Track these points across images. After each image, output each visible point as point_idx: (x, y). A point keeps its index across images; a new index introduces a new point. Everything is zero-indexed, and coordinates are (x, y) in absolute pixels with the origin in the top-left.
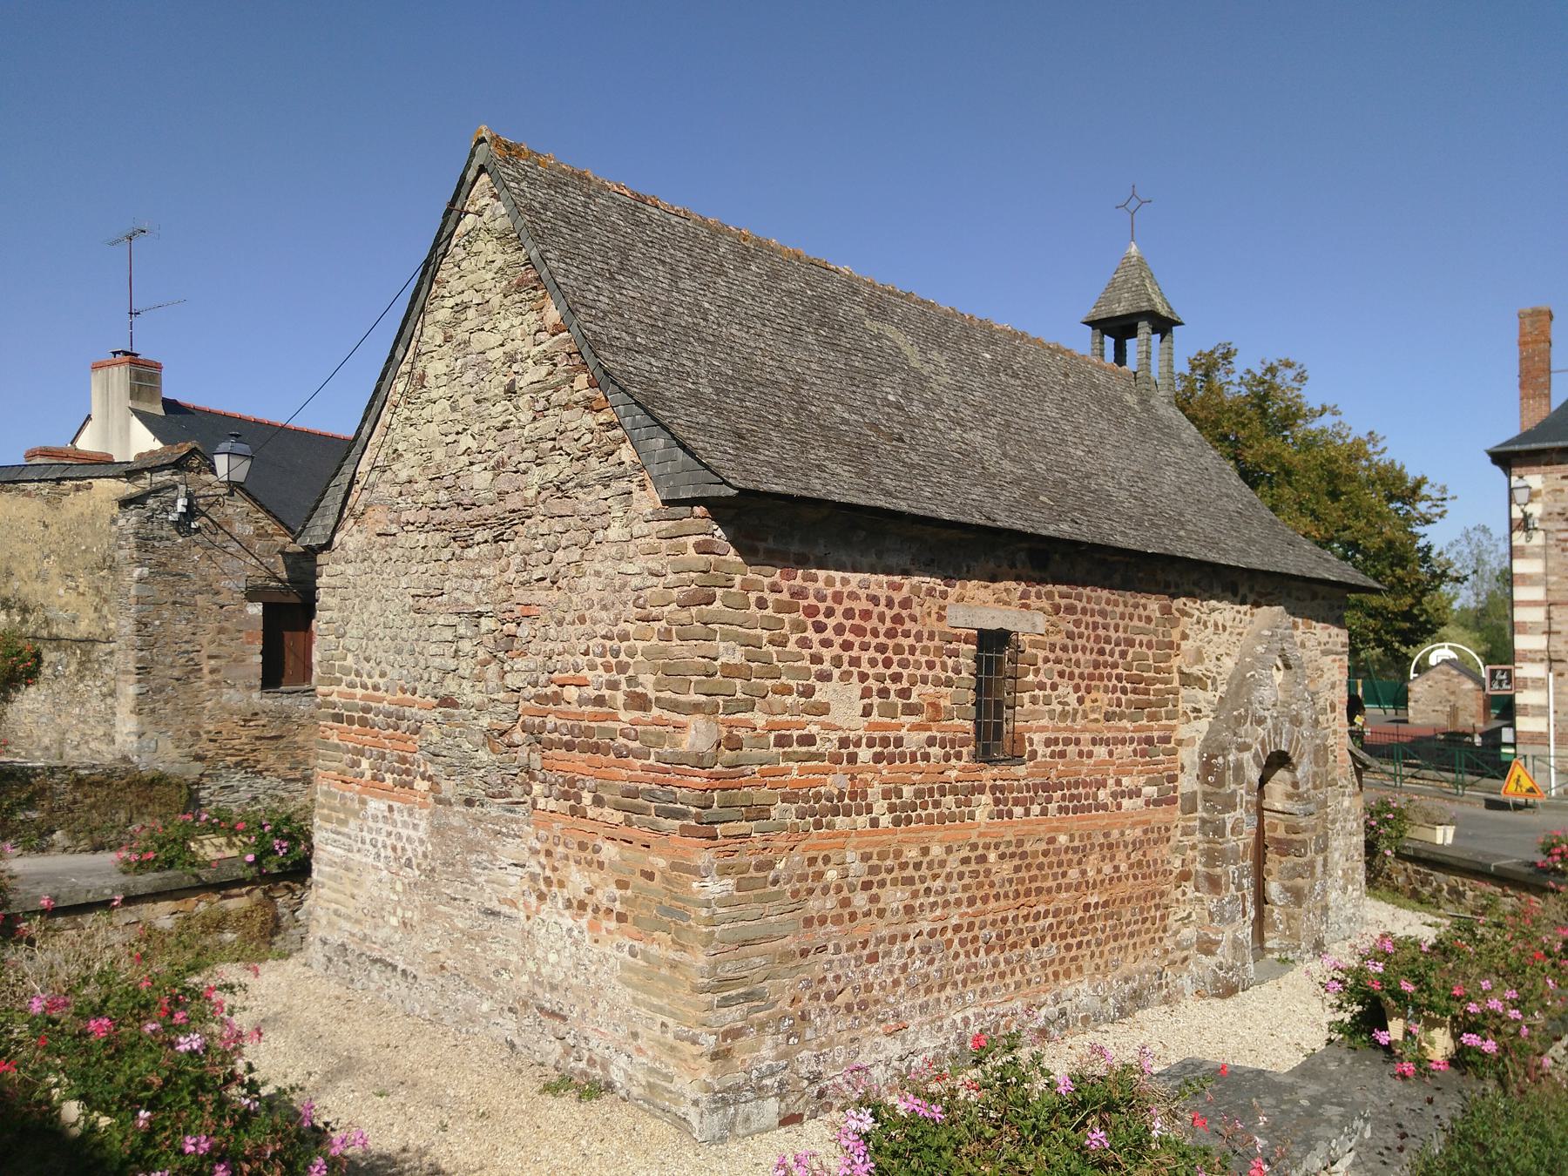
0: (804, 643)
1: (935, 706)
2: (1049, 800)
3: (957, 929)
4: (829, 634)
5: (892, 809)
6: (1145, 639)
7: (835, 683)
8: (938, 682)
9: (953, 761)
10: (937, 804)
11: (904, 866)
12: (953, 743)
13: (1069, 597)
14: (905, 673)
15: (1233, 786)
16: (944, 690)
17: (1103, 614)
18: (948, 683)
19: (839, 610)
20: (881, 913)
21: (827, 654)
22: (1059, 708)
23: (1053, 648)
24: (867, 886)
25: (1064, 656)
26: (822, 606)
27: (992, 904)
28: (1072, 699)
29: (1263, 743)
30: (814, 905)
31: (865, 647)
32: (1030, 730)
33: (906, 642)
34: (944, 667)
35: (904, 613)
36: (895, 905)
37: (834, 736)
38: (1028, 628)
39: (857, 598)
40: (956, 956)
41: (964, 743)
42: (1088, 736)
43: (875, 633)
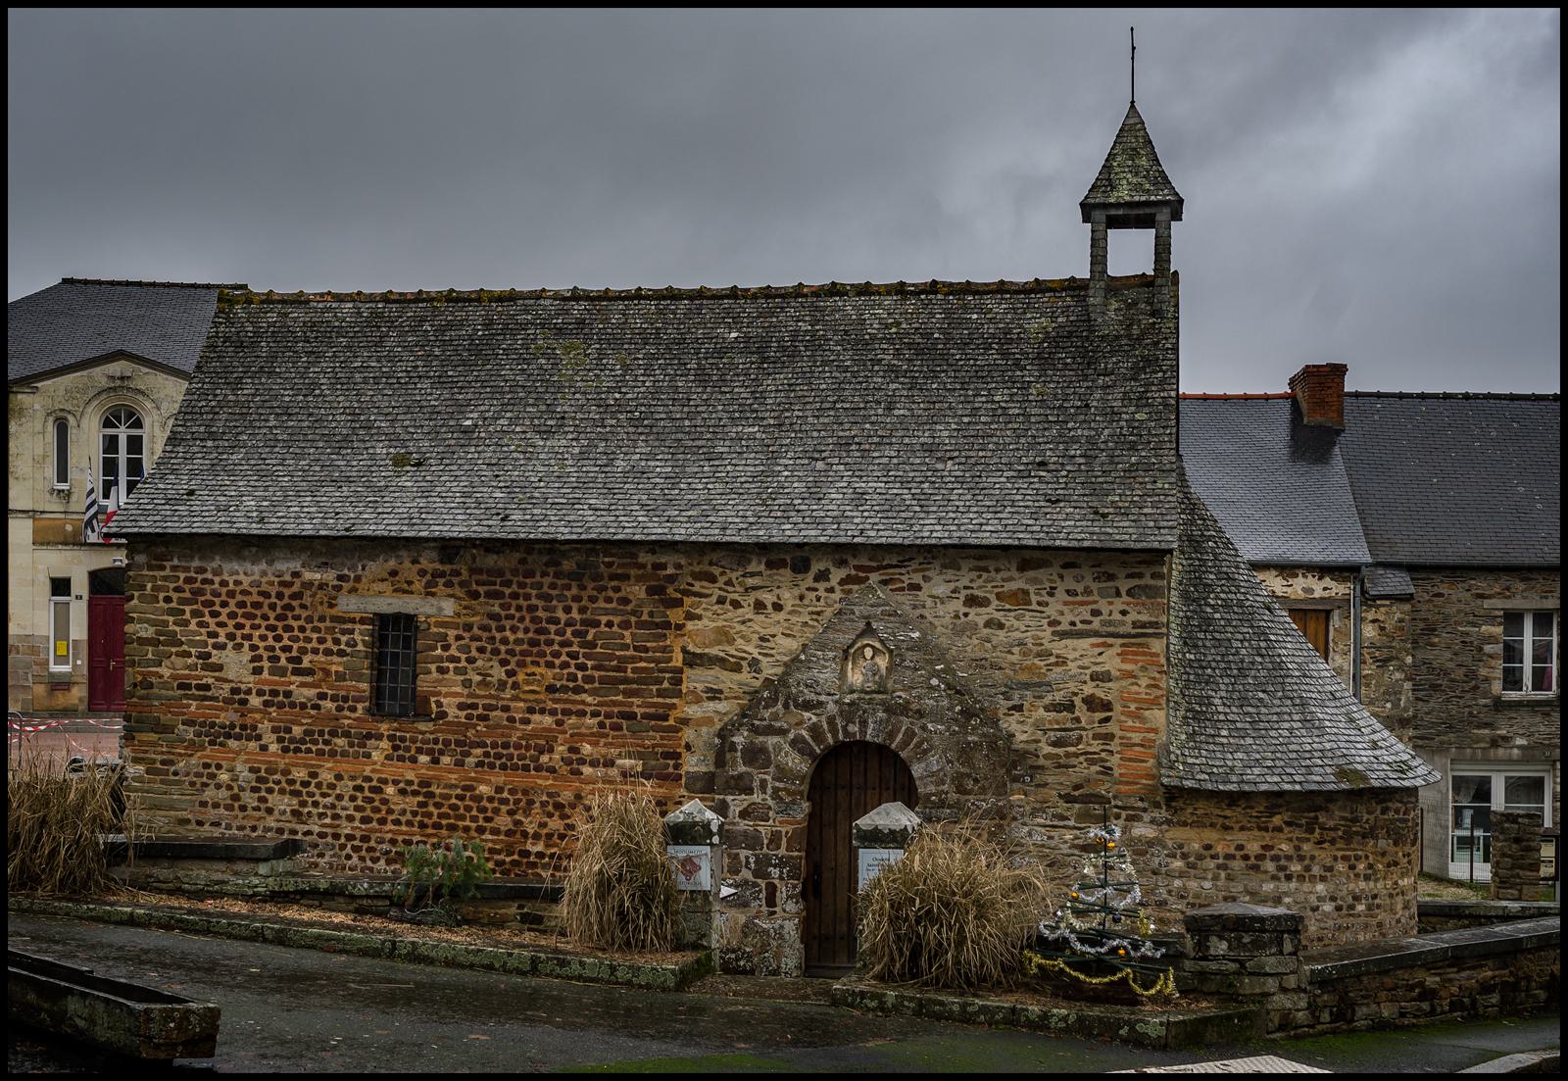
0: (200, 624)
1: (327, 673)
2: (468, 754)
3: (350, 837)
4: (223, 618)
5: (280, 740)
6: (616, 620)
7: (229, 651)
8: (328, 652)
9: (347, 713)
10: (326, 743)
11: (292, 782)
12: (345, 699)
14: (295, 646)
16: (335, 659)
17: (548, 598)
18: (341, 653)
19: (232, 602)
20: (270, 811)
23: (468, 627)
24: (255, 790)
25: (485, 635)
26: (217, 600)
27: (390, 826)
28: (498, 673)
29: (815, 730)
30: (209, 794)
31: (255, 627)
32: (439, 694)
33: (295, 624)
34: (337, 642)
35: (295, 603)
36: (282, 808)
37: (227, 686)
39: (250, 593)
40: (349, 857)
41: (357, 700)
43: (265, 617)
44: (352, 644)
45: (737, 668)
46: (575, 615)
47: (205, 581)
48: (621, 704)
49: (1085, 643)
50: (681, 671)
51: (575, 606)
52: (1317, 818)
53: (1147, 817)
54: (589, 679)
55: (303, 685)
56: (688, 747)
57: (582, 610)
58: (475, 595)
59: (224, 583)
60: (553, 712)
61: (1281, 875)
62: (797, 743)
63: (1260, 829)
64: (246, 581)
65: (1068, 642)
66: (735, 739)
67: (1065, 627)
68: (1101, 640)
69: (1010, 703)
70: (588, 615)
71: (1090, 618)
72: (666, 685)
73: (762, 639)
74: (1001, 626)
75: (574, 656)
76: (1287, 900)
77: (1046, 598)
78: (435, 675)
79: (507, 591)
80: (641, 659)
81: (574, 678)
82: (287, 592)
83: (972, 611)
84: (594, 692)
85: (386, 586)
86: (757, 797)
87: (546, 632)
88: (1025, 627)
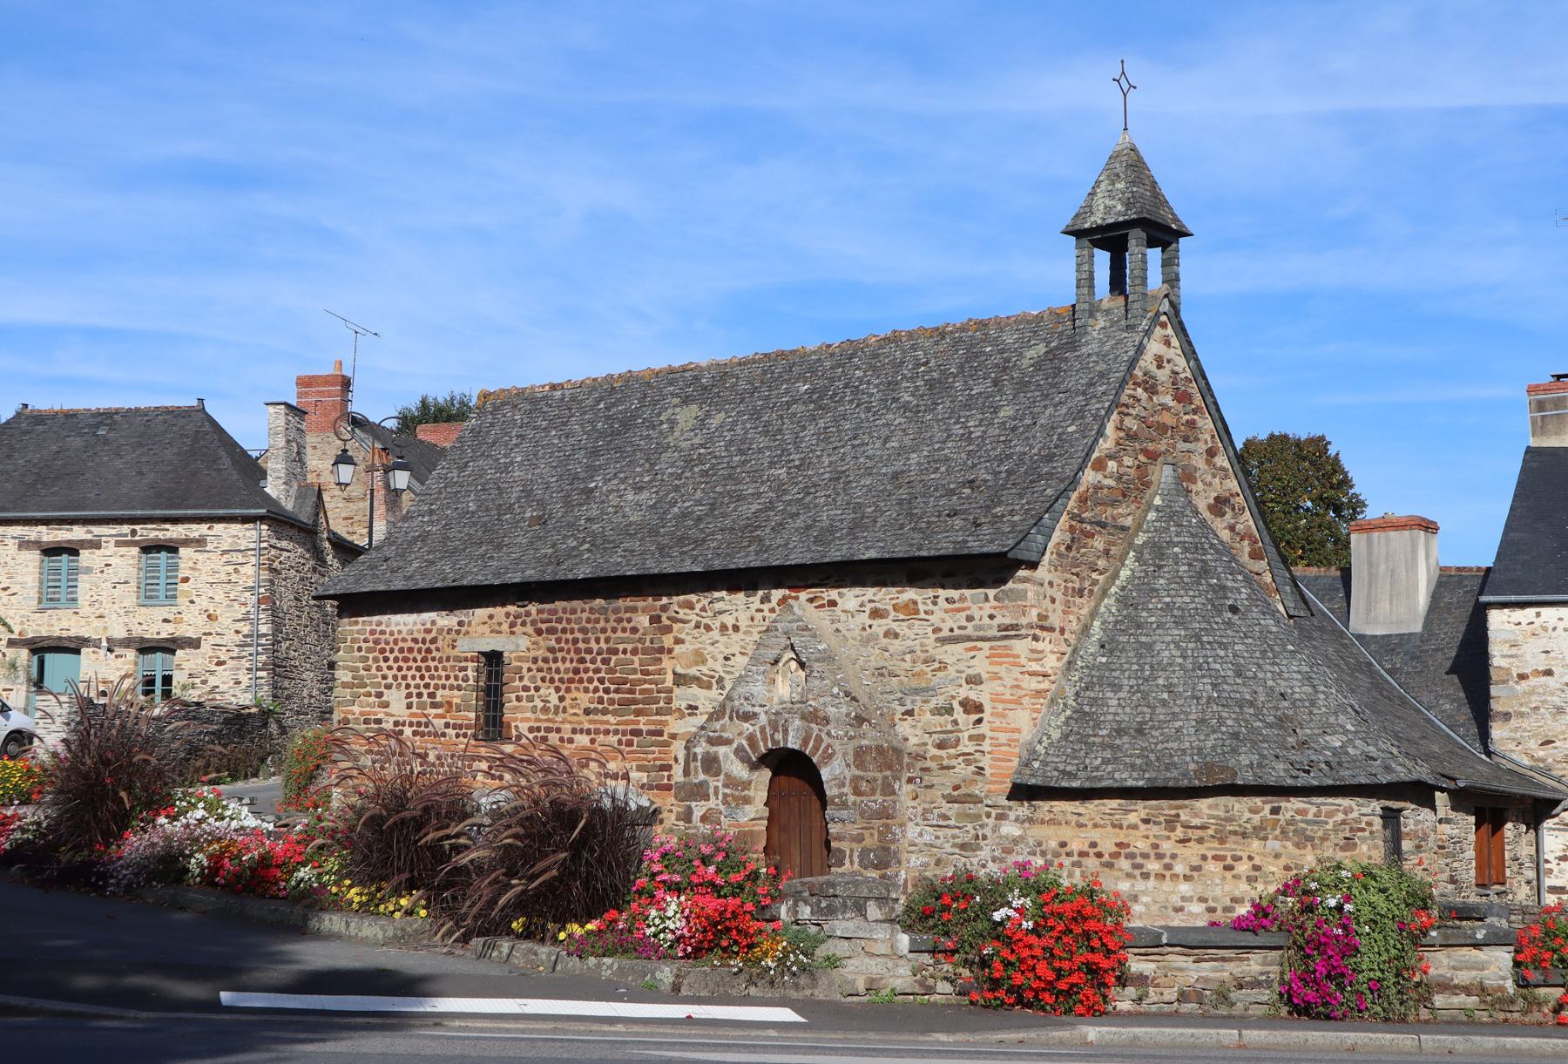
0: (379, 669)
1: (450, 704)
6: (629, 647)
8: (452, 688)
13: (550, 621)
15: (702, 777)
16: (456, 692)
17: (583, 631)
18: (459, 688)
21: (390, 674)
22: (540, 705)
23: (535, 660)
25: (545, 666)
29: (751, 739)
31: (409, 669)
32: (516, 720)
34: (456, 678)
35: (433, 647)
38: (512, 648)
42: (569, 727)
43: (415, 660)
44: (466, 679)
45: (709, 687)
46: (603, 645)
47: (382, 632)
48: (633, 722)
49: (960, 647)
50: (671, 691)
51: (602, 636)
52: (1178, 816)
53: (1012, 815)
54: (611, 701)
55: (436, 716)
56: (676, 760)
57: (607, 640)
58: (539, 632)
59: (392, 634)
60: (588, 732)
61: (1137, 872)
62: (739, 752)
63: (1114, 826)
64: (405, 629)
65: (948, 647)
66: (699, 750)
67: (945, 633)
68: (972, 644)
69: (903, 709)
70: (611, 645)
71: (964, 623)
72: (662, 704)
73: (726, 659)
74: (896, 636)
75: (601, 681)
76: (1144, 899)
77: (931, 607)
78: (515, 703)
79: (560, 627)
80: (646, 682)
81: (601, 701)
82: (429, 637)
83: (875, 623)
84: (615, 713)
85: (486, 629)
86: (712, 803)
87: (582, 661)
88: (915, 634)
